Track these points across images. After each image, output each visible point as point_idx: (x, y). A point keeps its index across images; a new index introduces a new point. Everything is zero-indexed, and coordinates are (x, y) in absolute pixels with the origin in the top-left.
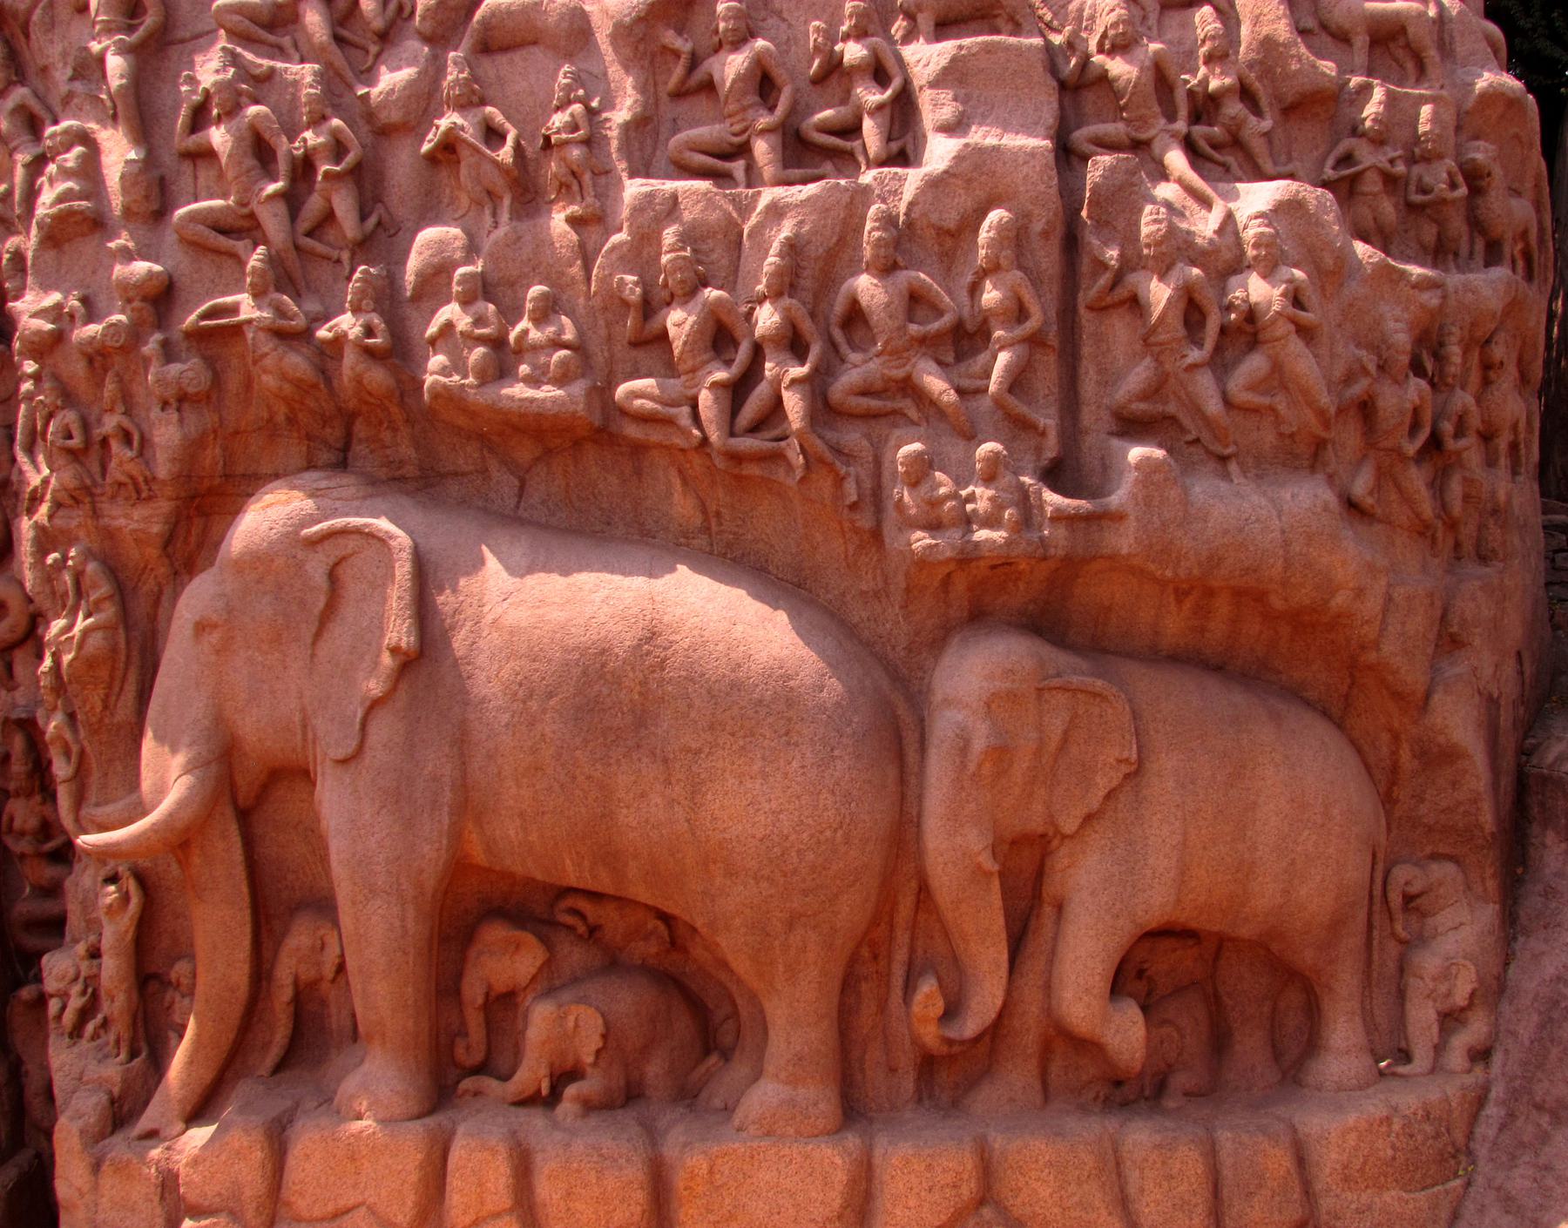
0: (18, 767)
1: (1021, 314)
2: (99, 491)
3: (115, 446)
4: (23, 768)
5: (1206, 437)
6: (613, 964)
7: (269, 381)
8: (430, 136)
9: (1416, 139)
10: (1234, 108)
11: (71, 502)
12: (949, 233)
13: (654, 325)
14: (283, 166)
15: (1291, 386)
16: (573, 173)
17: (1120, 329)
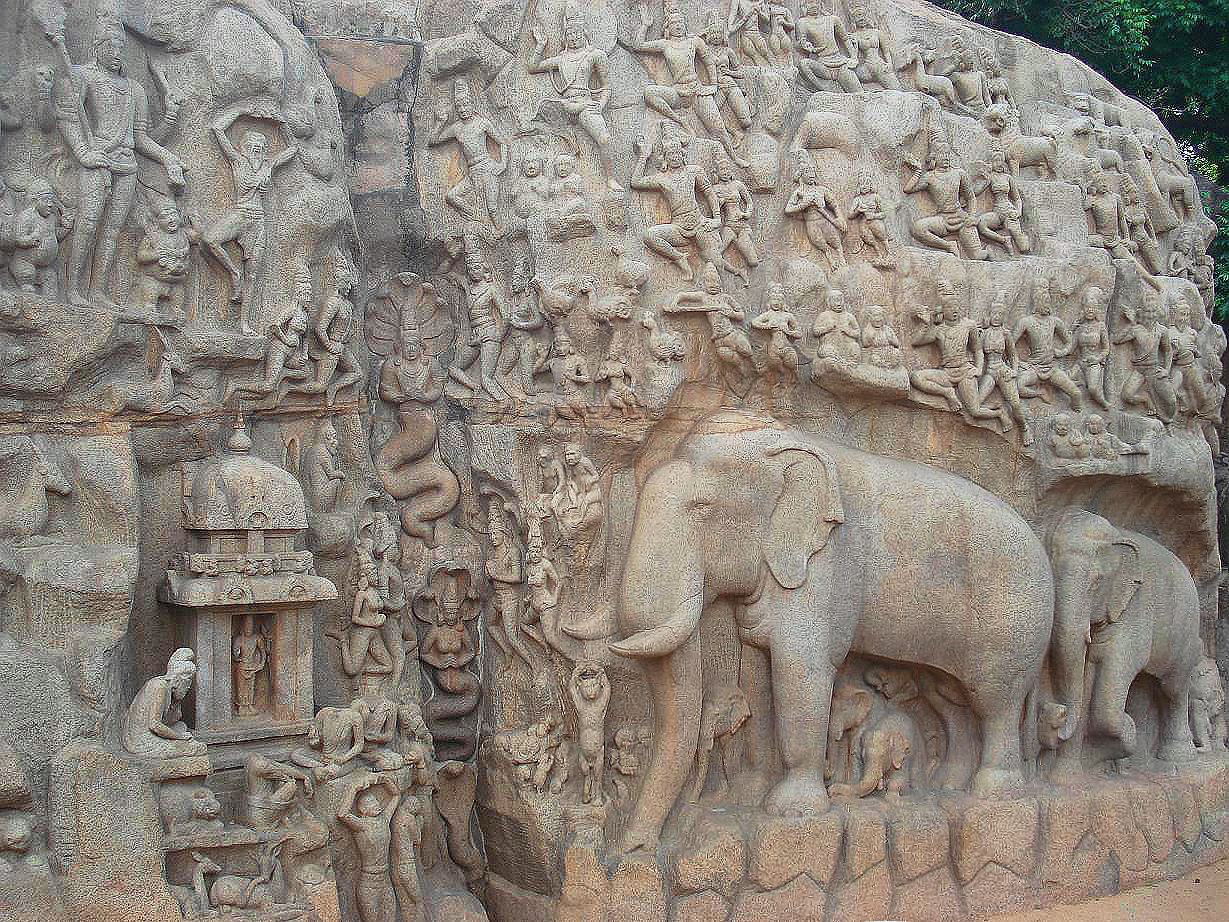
0: (451, 605)
1: (1102, 345)
2: (592, 410)
3: (617, 384)
4: (457, 605)
5: (1160, 414)
6: (889, 712)
7: (724, 351)
8: (792, 200)
9: (1196, 254)
10: (1144, 233)
11: (573, 415)
12: (1067, 297)
13: (931, 337)
14: (717, 209)
15: (1190, 388)
16: (877, 237)
17: (1124, 356)
